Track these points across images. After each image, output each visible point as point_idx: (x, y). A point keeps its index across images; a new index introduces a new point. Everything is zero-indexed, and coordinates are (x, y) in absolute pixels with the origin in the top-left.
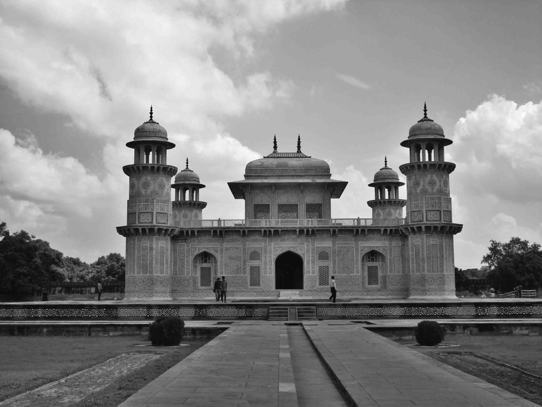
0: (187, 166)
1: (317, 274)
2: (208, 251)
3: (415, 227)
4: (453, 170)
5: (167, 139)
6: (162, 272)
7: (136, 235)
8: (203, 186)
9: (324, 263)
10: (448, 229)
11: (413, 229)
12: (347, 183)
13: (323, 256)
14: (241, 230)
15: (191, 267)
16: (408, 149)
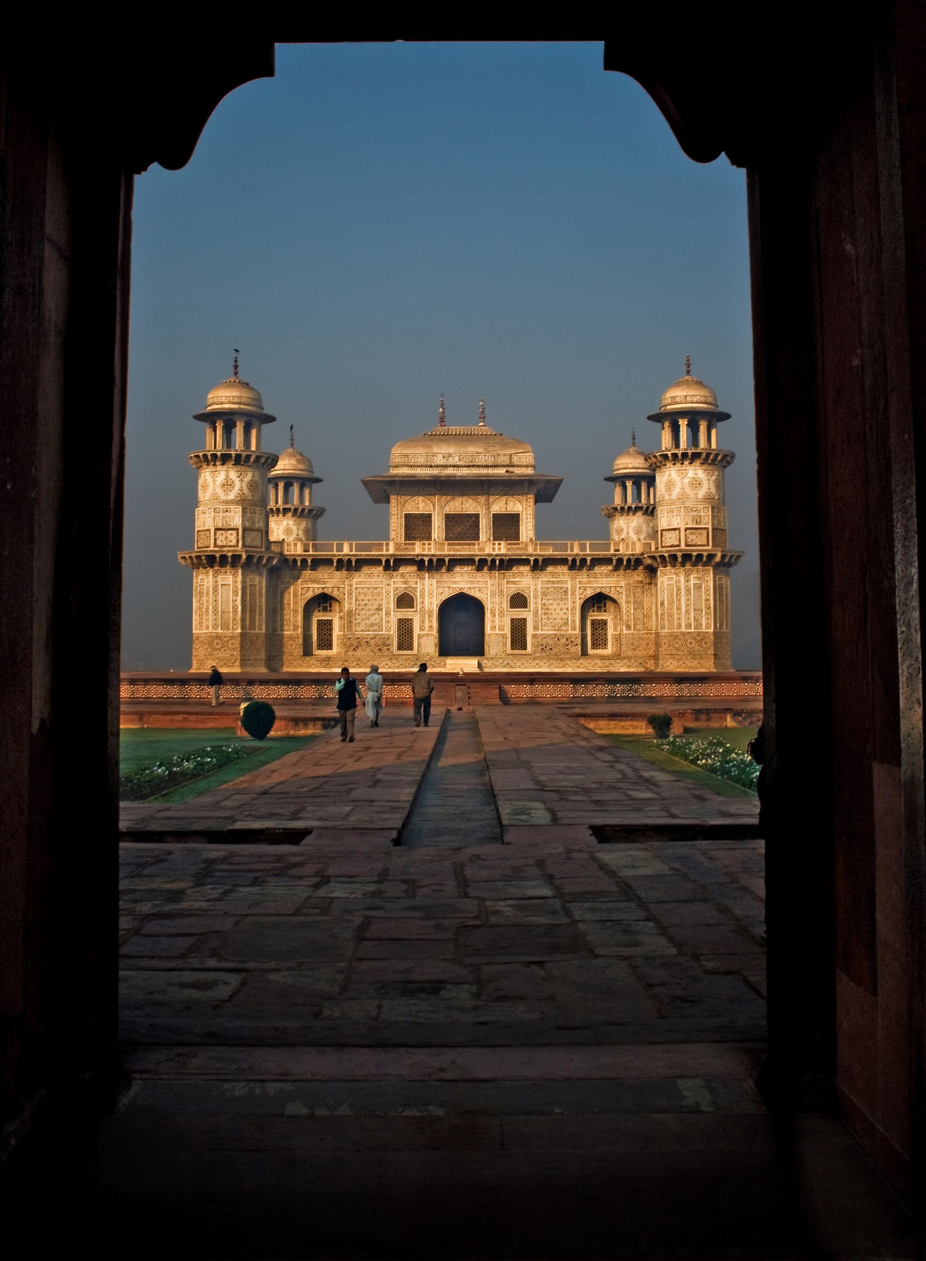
0: (292, 445)
1: (507, 631)
2: (328, 591)
3: (666, 555)
4: (729, 463)
5: (263, 409)
6: (252, 626)
7: (212, 567)
8: (318, 480)
9: (519, 613)
10: (718, 559)
11: (662, 557)
12: (562, 480)
13: (519, 601)
14: (384, 559)
15: (300, 618)
16: (660, 424)
